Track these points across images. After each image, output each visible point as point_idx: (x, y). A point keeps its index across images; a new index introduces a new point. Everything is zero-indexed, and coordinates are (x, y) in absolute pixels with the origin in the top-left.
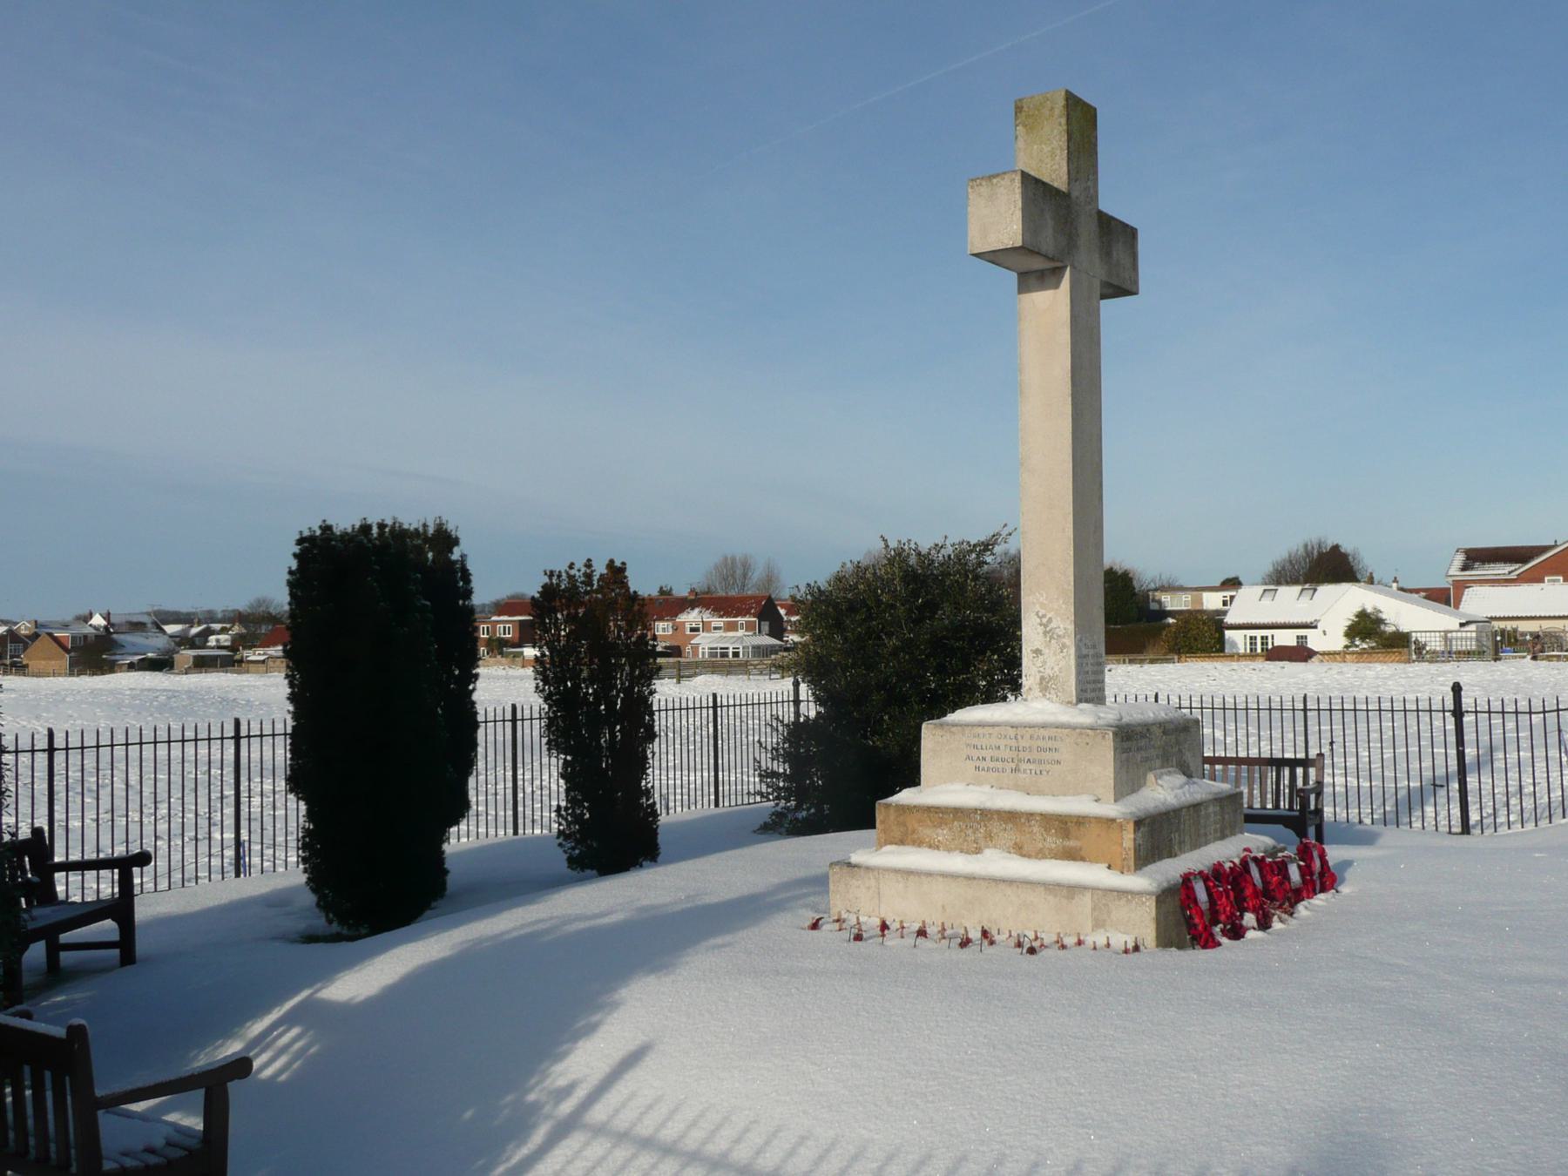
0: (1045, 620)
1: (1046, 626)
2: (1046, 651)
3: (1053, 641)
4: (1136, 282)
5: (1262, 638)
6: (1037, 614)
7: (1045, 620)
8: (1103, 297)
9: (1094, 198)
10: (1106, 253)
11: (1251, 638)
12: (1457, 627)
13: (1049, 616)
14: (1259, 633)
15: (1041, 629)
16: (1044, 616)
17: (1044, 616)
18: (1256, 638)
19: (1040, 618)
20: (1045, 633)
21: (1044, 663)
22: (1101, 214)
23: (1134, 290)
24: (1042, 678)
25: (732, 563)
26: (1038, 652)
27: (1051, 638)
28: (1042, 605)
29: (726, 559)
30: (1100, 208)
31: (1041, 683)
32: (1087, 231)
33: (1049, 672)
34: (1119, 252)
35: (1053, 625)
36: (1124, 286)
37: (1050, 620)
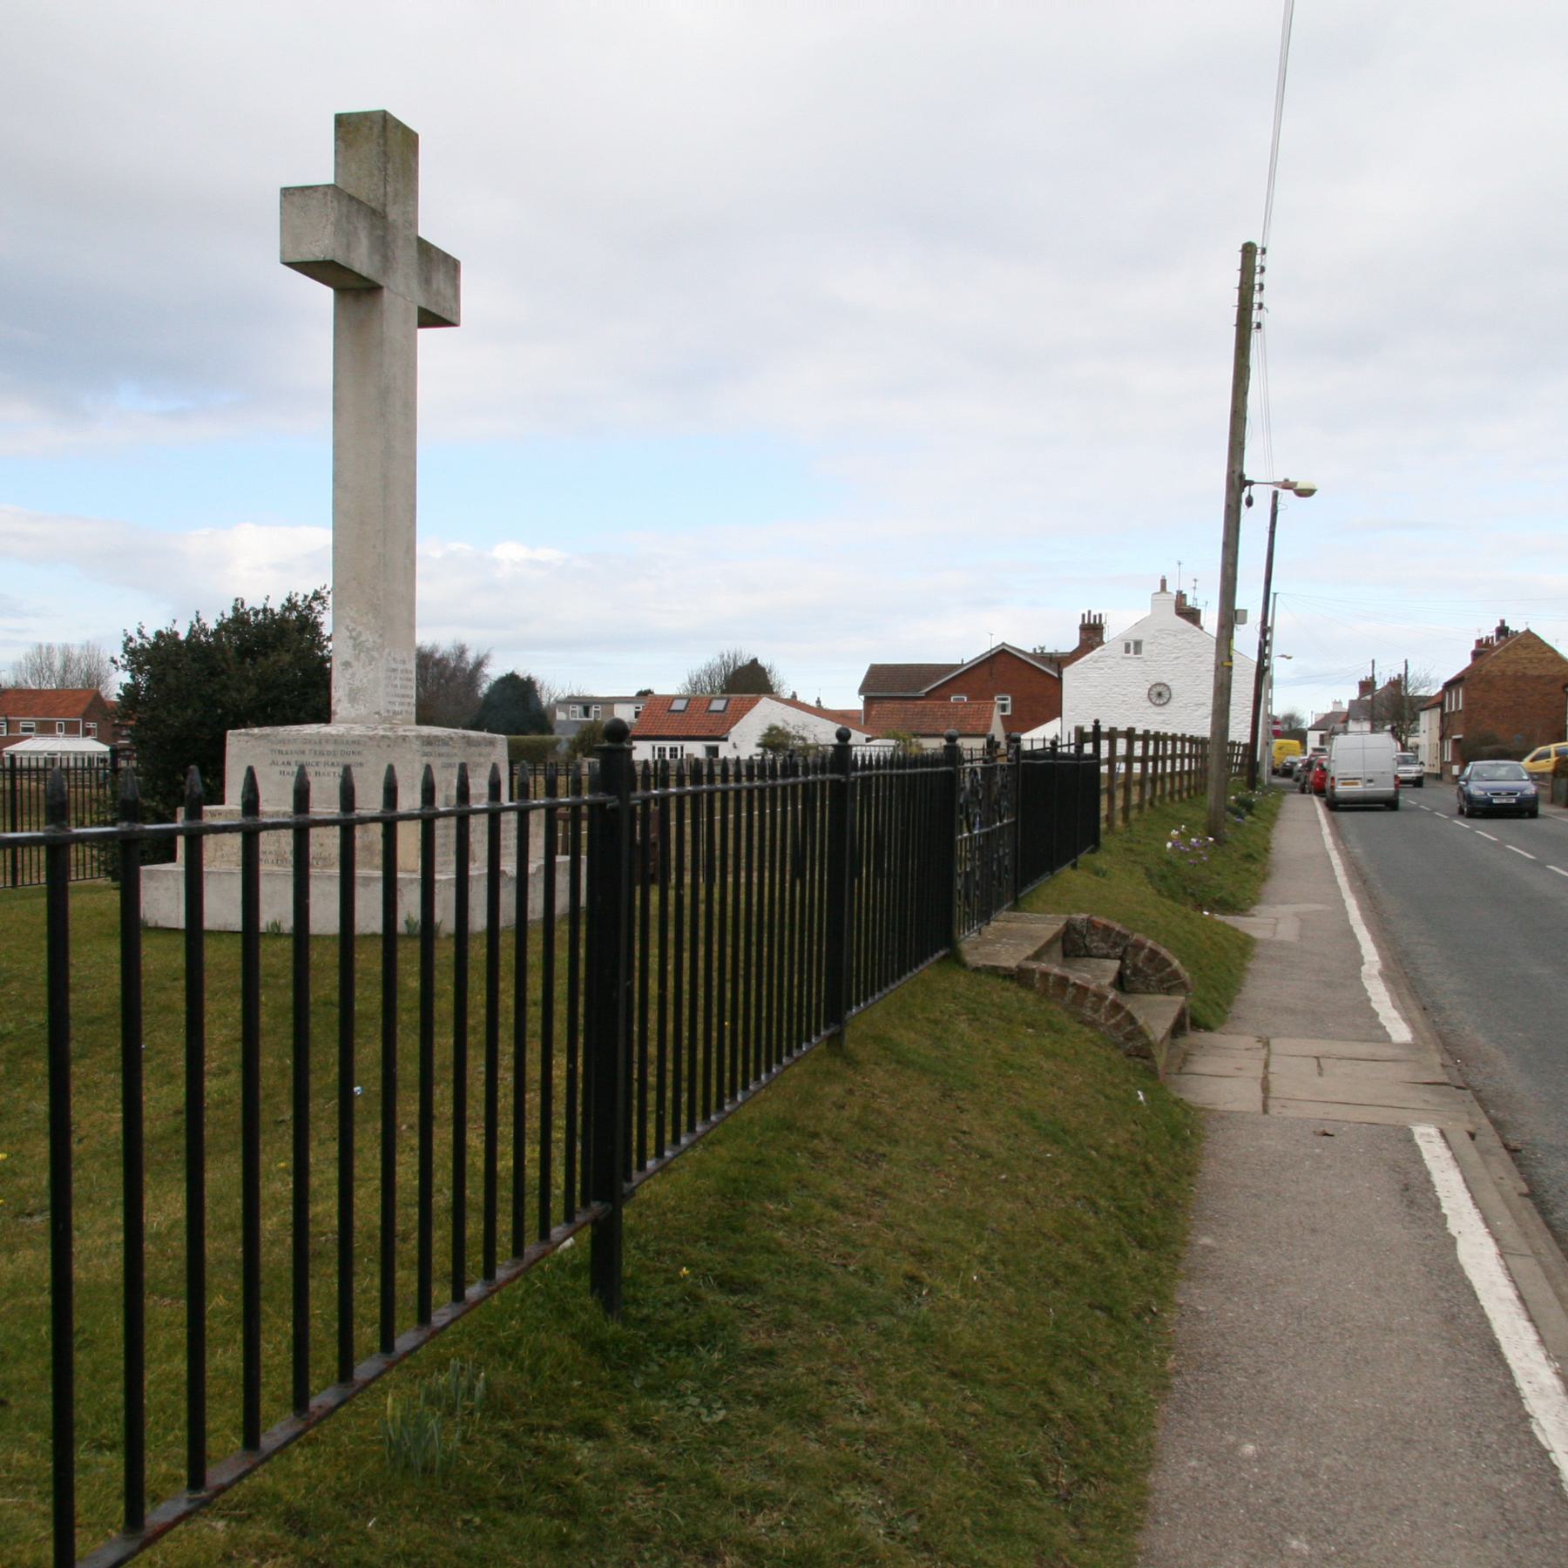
0: (354, 634)
1: (355, 639)
2: (355, 663)
3: (362, 655)
4: (458, 313)
5: (671, 749)
6: (347, 628)
7: (354, 634)
8: (422, 324)
9: (413, 224)
10: (427, 281)
11: (660, 749)
12: (864, 742)
13: (359, 629)
14: (668, 745)
15: (350, 643)
16: (354, 630)
17: (354, 630)
18: (664, 749)
19: (350, 631)
20: (355, 647)
21: (353, 675)
22: (421, 241)
23: (454, 320)
24: (351, 690)
25: (48, 653)
26: (347, 664)
27: (360, 651)
28: (353, 620)
29: (40, 647)
30: (421, 234)
31: (349, 695)
32: (406, 258)
33: (357, 683)
34: (439, 280)
35: (363, 639)
36: (444, 316)
37: (360, 634)
